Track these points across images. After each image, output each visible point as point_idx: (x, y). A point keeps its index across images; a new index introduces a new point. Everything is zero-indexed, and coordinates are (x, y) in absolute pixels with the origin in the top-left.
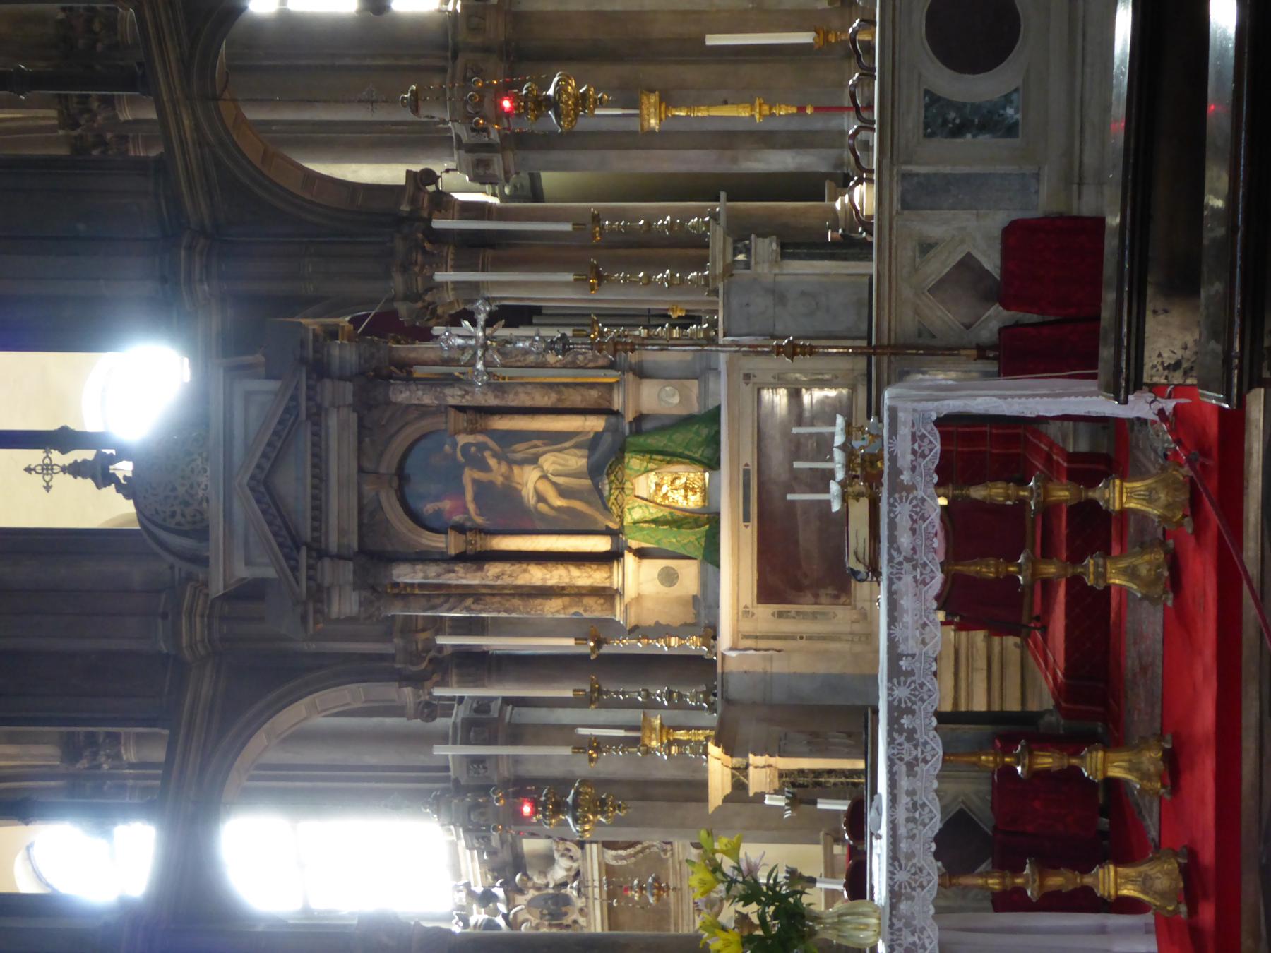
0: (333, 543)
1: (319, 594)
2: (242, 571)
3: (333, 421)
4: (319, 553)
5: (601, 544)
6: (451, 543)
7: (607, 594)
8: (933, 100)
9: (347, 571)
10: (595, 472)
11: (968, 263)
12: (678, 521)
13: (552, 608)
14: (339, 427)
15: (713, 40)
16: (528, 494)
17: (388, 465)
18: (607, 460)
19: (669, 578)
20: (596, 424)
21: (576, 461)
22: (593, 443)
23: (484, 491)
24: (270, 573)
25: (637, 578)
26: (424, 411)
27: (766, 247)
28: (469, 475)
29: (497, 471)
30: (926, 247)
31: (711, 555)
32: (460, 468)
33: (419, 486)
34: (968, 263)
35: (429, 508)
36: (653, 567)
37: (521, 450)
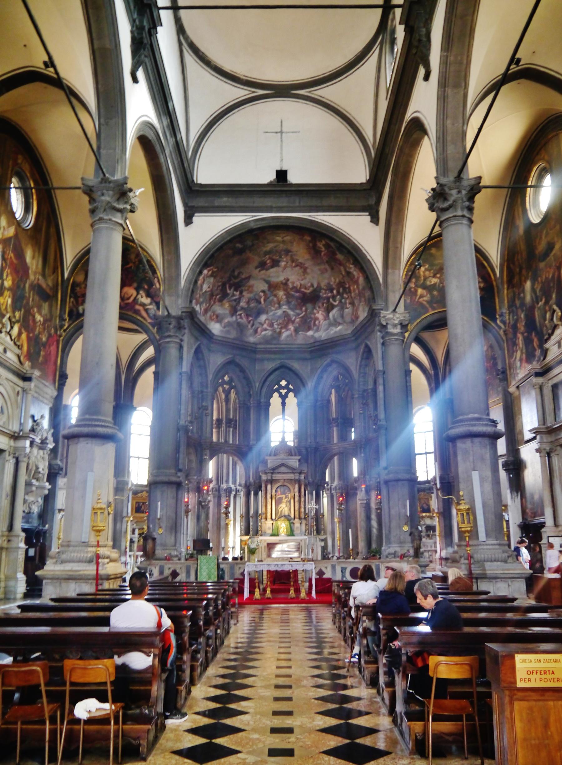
0: (274, 475)
1: (266, 473)
2: (269, 461)
3: (292, 475)
4: (272, 473)
5: (274, 517)
6: (274, 494)
7: (266, 519)
8: (346, 569)
9: (269, 478)
10: (285, 516)
11: (324, 573)
12: (278, 529)
13: (264, 510)
14: (292, 476)
15: (350, 530)
16: (281, 505)
17: (286, 484)
18: (287, 518)
19: (269, 528)
20: (292, 516)
21: (286, 513)
22: (289, 516)
23: (281, 498)
24: (269, 466)
25: (269, 523)
26: (294, 489)
27: (323, 544)
28: (284, 496)
29: (284, 500)
30: (326, 568)
31: (272, 535)
32: (284, 493)
33: (282, 488)
34: (324, 573)
35: (279, 490)
36: (271, 526)
37: (288, 504)
